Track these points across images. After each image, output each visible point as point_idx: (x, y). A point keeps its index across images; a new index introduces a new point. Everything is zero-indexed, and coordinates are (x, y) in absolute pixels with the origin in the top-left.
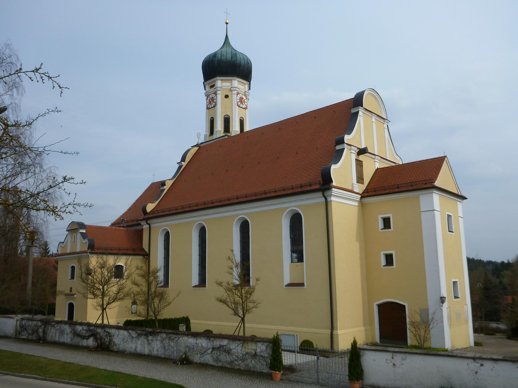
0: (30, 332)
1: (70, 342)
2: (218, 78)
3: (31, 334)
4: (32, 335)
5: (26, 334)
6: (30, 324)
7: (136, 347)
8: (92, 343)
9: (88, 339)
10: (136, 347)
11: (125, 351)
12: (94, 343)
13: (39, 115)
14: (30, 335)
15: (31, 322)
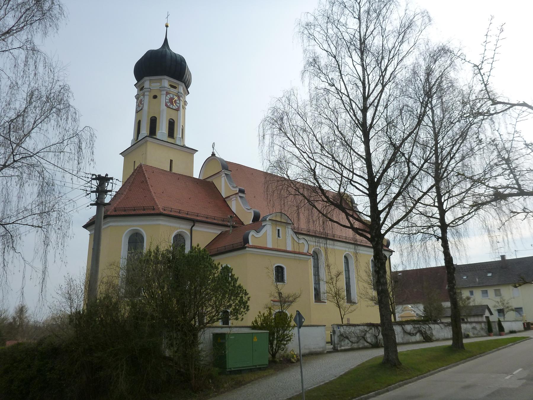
0: (354, 339)
1: (402, 342)
2: (166, 77)
3: (356, 342)
4: (357, 342)
5: (348, 343)
6: (352, 331)
7: (444, 334)
8: (419, 338)
9: (416, 335)
10: (444, 334)
11: (440, 339)
12: (420, 337)
13: (350, 57)
14: (355, 343)
15: (353, 328)
